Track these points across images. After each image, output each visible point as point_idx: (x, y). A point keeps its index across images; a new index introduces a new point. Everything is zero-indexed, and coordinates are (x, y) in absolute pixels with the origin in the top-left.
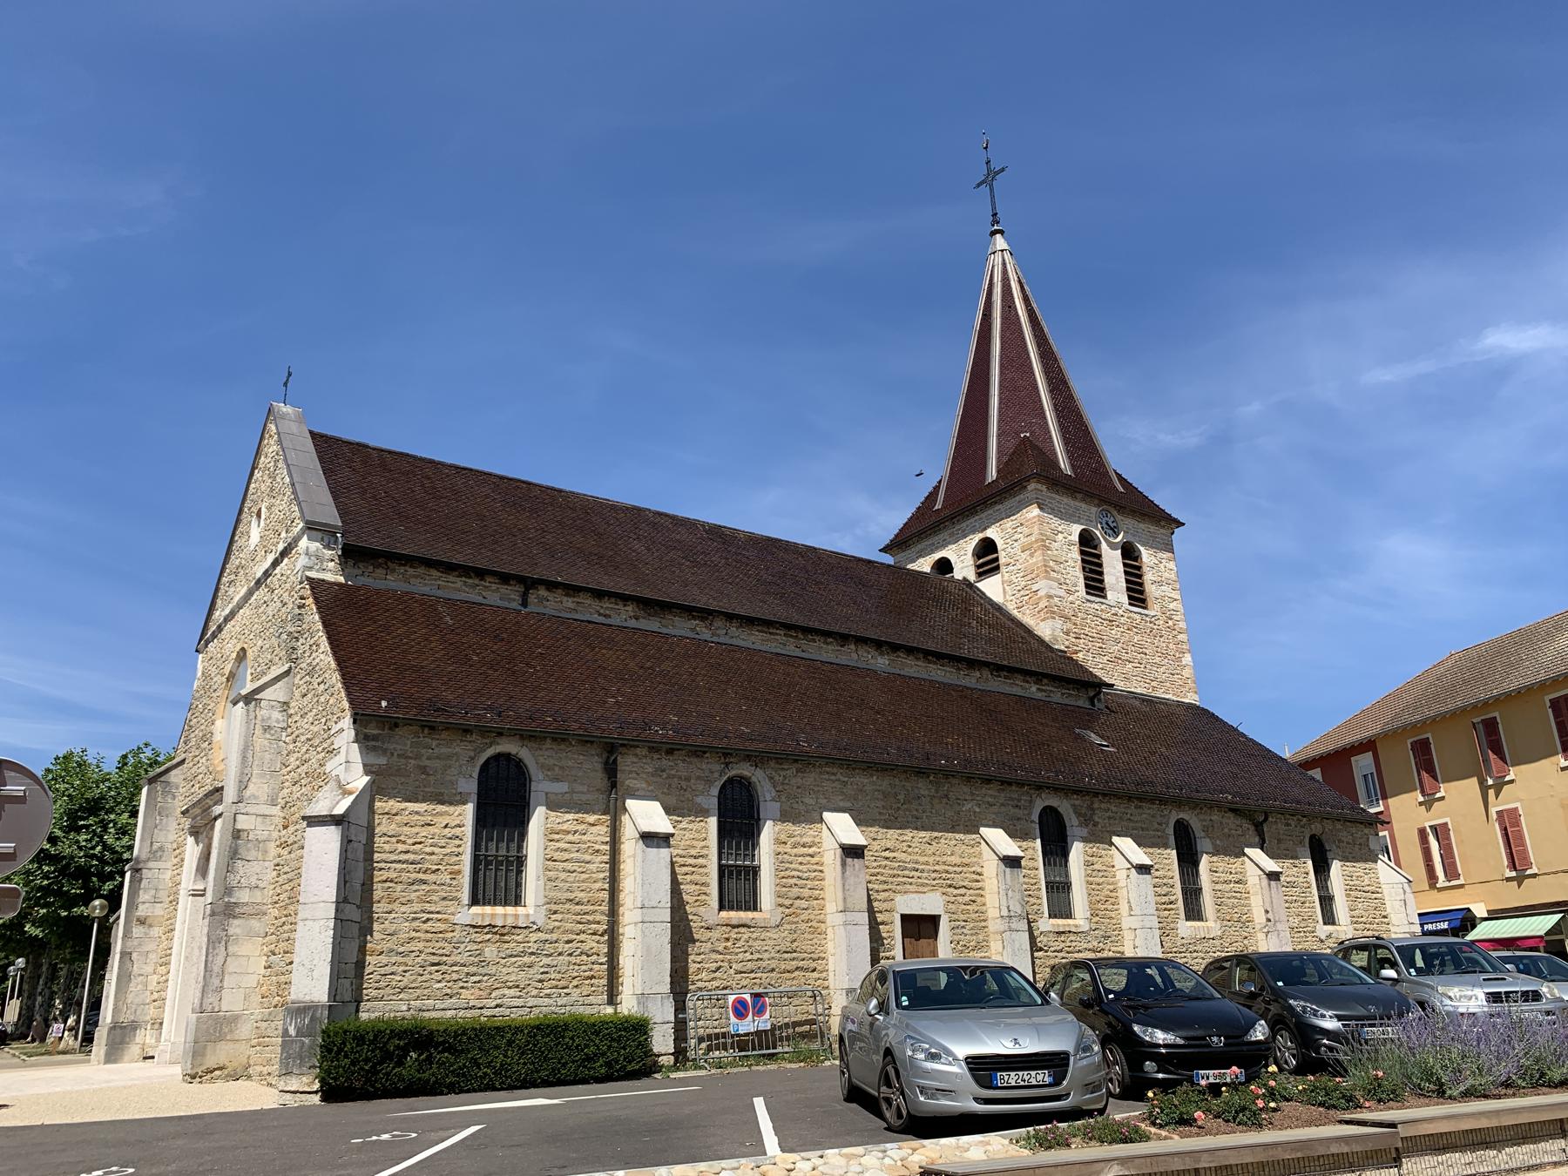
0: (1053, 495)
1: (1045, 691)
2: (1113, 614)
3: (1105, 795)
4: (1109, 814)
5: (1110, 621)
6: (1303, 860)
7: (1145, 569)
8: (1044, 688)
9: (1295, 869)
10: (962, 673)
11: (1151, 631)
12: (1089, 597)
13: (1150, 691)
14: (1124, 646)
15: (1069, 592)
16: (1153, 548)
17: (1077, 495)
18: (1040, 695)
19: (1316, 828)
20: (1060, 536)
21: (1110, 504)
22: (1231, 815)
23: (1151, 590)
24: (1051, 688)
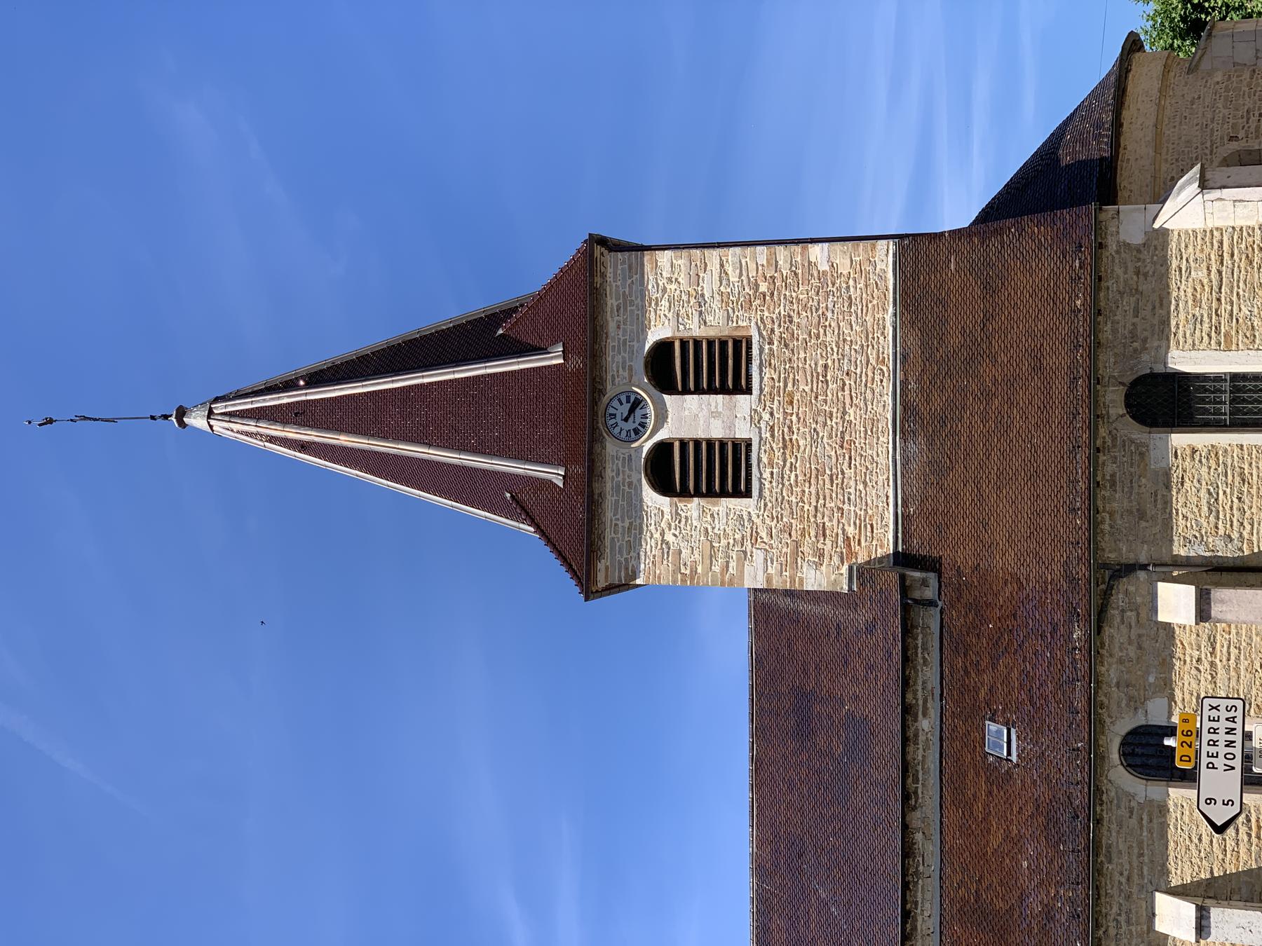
0: (607, 542)
1: (925, 701)
2: (773, 436)
3: (1097, 925)
4: (1122, 919)
5: (785, 447)
6: (1171, 459)
7: (685, 334)
8: (921, 702)
9: (1187, 484)
10: (921, 868)
11: (786, 346)
12: (755, 492)
13: (885, 369)
14: (821, 419)
15: (755, 536)
16: (643, 306)
17: (597, 492)
18: (934, 712)
19: (1114, 400)
20: (669, 537)
21: (594, 414)
22: (1107, 631)
23: (715, 325)
24: (920, 688)
